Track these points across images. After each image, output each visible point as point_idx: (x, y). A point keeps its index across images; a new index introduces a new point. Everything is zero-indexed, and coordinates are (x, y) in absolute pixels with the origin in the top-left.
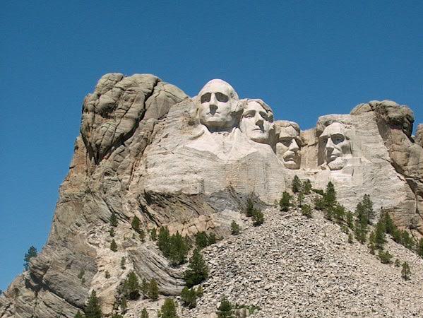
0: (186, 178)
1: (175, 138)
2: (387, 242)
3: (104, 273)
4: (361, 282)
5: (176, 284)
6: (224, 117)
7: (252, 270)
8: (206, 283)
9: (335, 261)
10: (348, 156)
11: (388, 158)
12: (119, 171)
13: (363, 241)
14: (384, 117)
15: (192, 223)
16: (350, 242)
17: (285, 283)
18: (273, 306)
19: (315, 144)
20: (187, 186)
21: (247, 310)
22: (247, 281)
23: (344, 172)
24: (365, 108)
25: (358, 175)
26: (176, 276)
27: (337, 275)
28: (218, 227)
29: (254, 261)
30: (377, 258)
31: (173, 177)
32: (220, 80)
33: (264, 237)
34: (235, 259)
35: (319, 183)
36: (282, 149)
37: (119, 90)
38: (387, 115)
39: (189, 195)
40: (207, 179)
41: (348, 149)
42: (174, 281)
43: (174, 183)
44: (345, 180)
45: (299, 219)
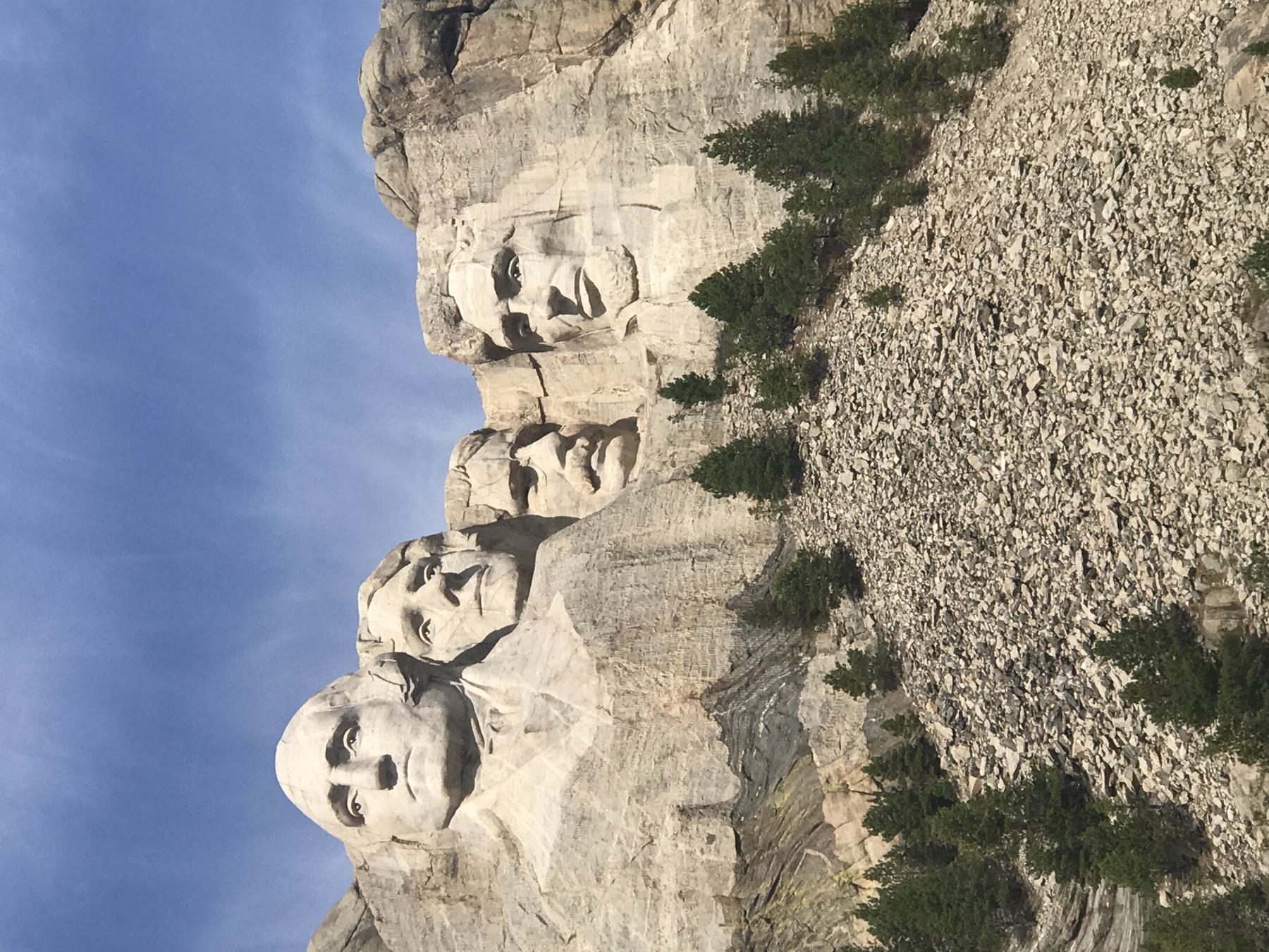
0: (669, 883)
1: (514, 930)
2: (922, 47)
4: (1083, 133)
5: (1109, 912)
6: (425, 730)
7: (1041, 591)
8: (1101, 780)
9: (1000, 252)
10: (582, 227)
11: (586, 69)
13: (920, 146)
14: (421, 88)
15: (856, 852)
16: (919, 194)
17: (1094, 447)
18: (1190, 489)
19: (536, 366)
20: (702, 873)
21: (1209, 601)
22: (1087, 612)
23: (645, 240)
24: (392, 169)
25: (654, 184)
26: (1073, 914)
27: (1057, 234)
28: (870, 742)
29: (1008, 586)
30: (987, 79)
31: (666, 933)
33: (909, 549)
34: (1001, 664)
35: (691, 340)
36: (558, 500)
38: (413, 77)
39: (743, 870)
40: (677, 795)
41: (553, 231)
42: (1096, 921)
43: (692, 931)
44: (673, 236)
45: (831, 408)
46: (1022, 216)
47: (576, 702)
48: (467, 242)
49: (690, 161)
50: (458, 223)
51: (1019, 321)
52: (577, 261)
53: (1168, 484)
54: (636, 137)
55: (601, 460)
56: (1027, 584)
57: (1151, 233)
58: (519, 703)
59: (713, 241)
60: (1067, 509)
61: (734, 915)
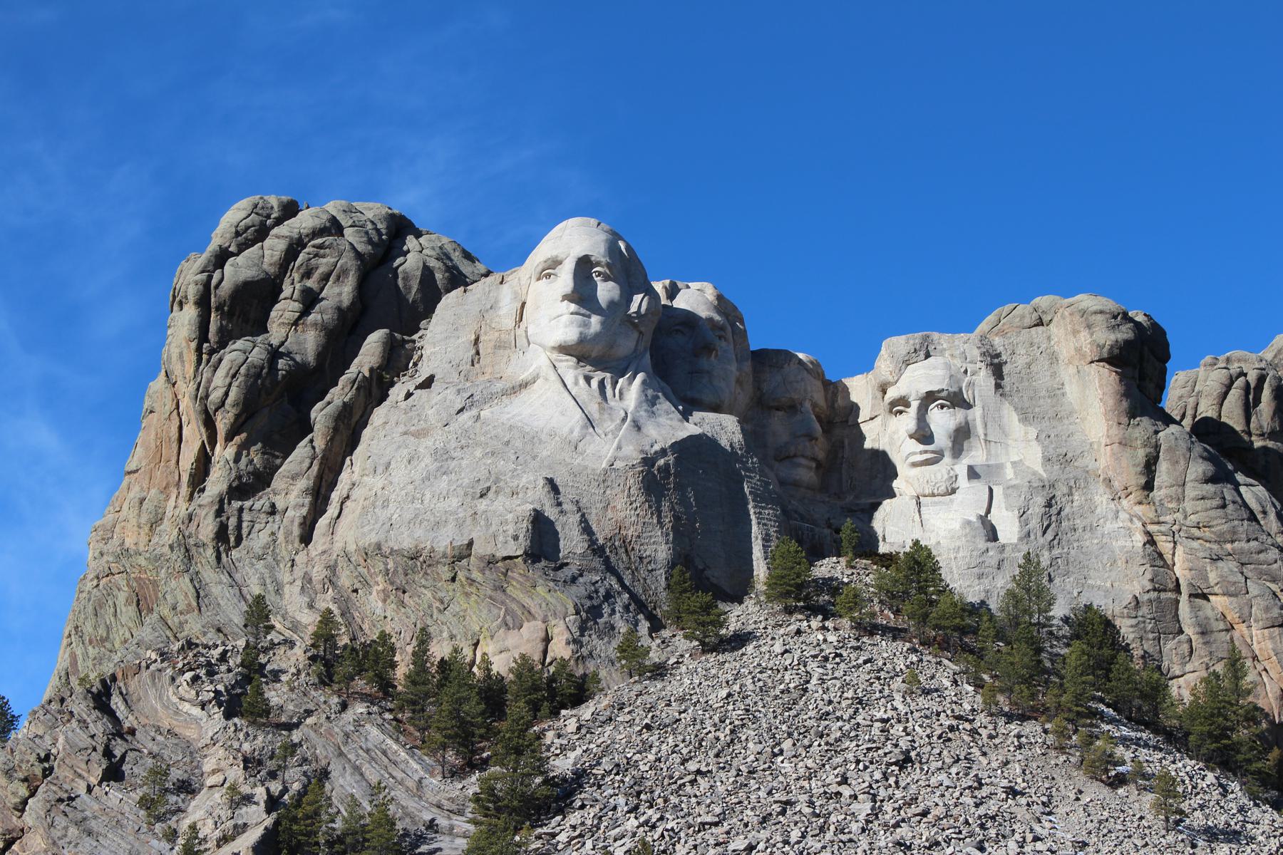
3: (218, 796)
8: (545, 830)
12: (278, 482)
24: (1023, 317)
25: (1005, 513)
32: (593, 221)
33: (724, 693)
37: (281, 246)
38: (1092, 335)
39: (491, 562)
46: (970, 787)
47: (620, 441)
48: (966, 372)
49: (1021, 539)
50: (979, 365)
51: (892, 780)
52: (947, 454)
54: (1040, 500)
55: (799, 465)
56: (696, 780)
59: (961, 555)
61: (456, 553)
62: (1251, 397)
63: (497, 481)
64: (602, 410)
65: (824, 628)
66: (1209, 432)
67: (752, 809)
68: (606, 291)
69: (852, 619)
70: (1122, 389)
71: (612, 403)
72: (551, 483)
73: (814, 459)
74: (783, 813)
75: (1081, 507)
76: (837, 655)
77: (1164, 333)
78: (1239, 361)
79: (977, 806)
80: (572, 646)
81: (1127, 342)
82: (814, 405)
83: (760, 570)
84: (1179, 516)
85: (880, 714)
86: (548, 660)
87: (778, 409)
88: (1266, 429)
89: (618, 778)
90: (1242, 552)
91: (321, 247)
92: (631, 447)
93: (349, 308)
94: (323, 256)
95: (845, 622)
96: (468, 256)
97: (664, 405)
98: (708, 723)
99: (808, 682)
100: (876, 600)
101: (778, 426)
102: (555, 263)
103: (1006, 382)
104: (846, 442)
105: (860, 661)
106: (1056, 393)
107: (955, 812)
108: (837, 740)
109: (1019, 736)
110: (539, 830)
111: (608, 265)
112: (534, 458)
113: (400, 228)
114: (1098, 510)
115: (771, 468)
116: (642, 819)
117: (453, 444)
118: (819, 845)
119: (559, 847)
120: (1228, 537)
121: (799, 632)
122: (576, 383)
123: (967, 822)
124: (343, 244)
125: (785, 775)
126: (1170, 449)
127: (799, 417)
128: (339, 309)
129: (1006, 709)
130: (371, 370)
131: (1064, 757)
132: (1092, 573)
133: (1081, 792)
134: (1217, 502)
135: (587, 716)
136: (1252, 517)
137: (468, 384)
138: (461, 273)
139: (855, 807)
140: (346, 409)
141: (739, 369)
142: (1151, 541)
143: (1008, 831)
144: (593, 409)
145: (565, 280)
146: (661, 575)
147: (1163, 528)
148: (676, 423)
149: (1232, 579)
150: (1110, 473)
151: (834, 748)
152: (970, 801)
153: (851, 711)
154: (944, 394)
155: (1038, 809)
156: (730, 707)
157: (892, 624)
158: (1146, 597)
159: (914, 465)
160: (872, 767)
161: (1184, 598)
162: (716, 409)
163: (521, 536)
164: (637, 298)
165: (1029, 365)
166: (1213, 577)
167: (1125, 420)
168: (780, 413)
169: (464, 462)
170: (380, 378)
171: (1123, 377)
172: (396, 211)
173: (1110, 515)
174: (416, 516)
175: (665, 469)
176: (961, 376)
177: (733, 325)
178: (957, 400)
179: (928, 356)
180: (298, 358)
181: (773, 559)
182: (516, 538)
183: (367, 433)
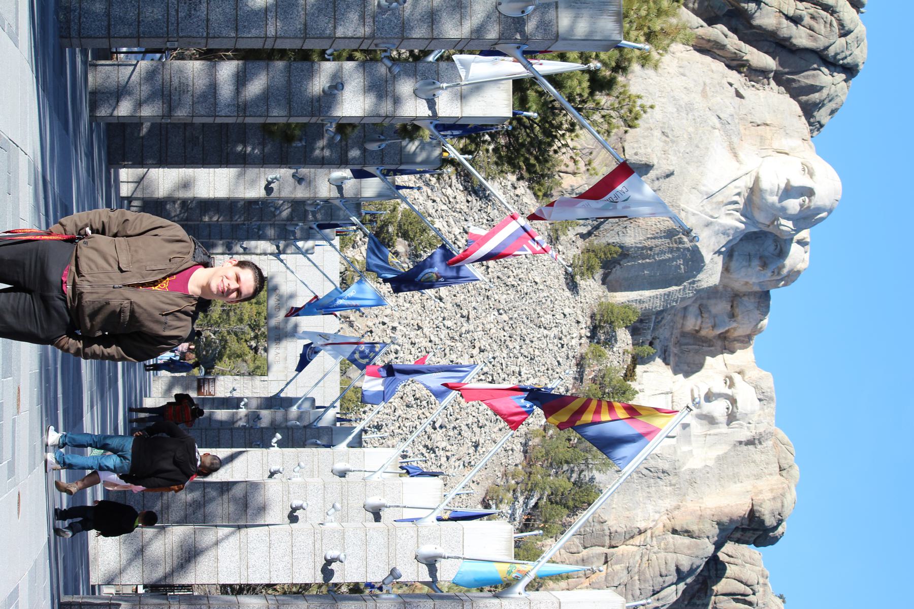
18: (408, 305)
24: (786, 458)
32: (839, 197)
50: (754, 431)
51: (483, 377)
53: (418, 307)
54: (666, 467)
57: (420, 412)
58: (727, 214)
60: (463, 296)
62: (739, 597)
63: (673, 142)
64: (719, 203)
65: (581, 337)
66: (714, 568)
67: (465, 299)
68: (793, 205)
69: (587, 354)
70: (735, 517)
71: (723, 209)
72: (672, 174)
73: (701, 328)
74: (462, 316)
75: (663, 491)
76: (563, 346)
77: (773, 544)
78: (764, 591)
79: (467, 425)
80: (570, 188)
81: (763, 522)
82: (735, 329)
83: (621, 297)
84: (656, 549)
85: (523, 371)
86: (561, 174)
87: (732, 306)
88: (718, 606)
89: (485, 221)
90: (633, 585)
91: (831, 25)
92: (694, 222)
93: (791, 43)
94: (825, 27)
95: (584, 350)
96: (833, 112)
97: (724, 240)
98: (519, 271)
99: (545, 328)
100: (601, 367)
101: (721, 307)
102: (811, 174)
103: (745, 448)
104: (712, 348)
105: (559, 359)
106: (736, 478)
107: (463, 412)
108: (507, 347)
109: (512, 450)
110: (454, 177)
111: (809, 207)
112: (687, 163)
113: (850, 71)
114: (660, 501)
115: (695, 302)
116: (459, 237)
117: (696, 114)
118: (442, 337)
119: (444, 190)
120: (642, 578)
121: (578, 322)
122: (736, 187)
123: (457, 419)
124: (834, 37)
125: (486, 316)
126: (697, 545)
127: (727, 319)
128: (790, 38)
129: (530, 443)
130: (747, 61)
131: (500, 475)
132: (622, 496)
133: (478, 484)
134: (664, 574)
135: (525, 200)
136: (655, 593)
137: (737, 121)
138: (820, 108)
139: (466, 357)
140: (723, 47)
141: (754, 283)
142: (640, 533)
143: (452, 442)
144: (719, 198)
145: (800, 180)
146: (616, 240)
147: (648, 539)
148: (712, 247)
149: (616, 578)
150: (682, 509)
151: (503, 344)
152: (470, 420)
153: (526, 354)
154: (735, 410)
155: (467, 459)
156: (529, 284)
157: (585, 377)
158: (606, 528)
159: (692, 391)
160: (491, 366)
161: (605, 550)
162: (726, 269)
163: (637, 157)
164: (790, 224)
165: (754, 462)
166: (617, 567)
167: (715, 519)
168: (729, 308)
169: (685, 121)
170: (743, 66)
171: (743, 518)
172: (861, 67)
173: (657, 509)
174: (650, 94)
175: (681, 242)
176: (747, 420)
177: (782, 280)
178: (731, 418)
179: (760, 400)
180: (757, 14)
181: (627, 306)
182: (636, 154)
183: (708, 59)
